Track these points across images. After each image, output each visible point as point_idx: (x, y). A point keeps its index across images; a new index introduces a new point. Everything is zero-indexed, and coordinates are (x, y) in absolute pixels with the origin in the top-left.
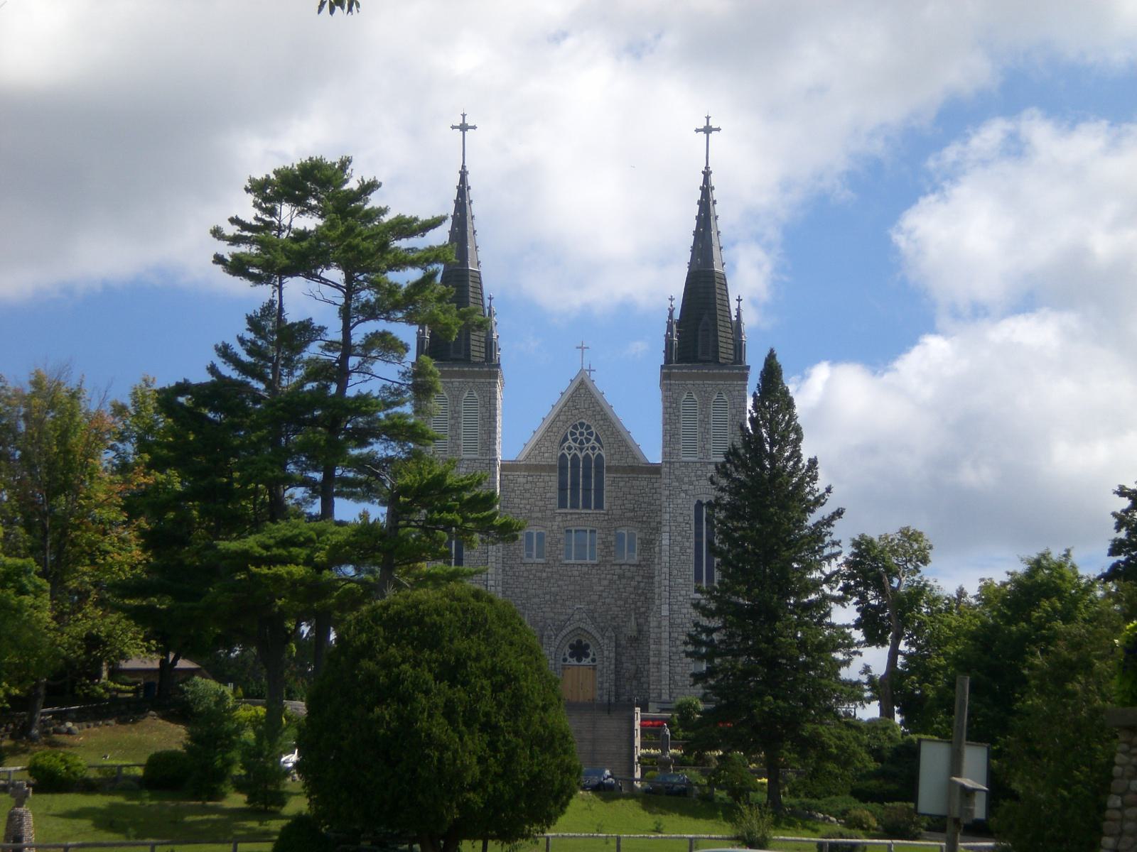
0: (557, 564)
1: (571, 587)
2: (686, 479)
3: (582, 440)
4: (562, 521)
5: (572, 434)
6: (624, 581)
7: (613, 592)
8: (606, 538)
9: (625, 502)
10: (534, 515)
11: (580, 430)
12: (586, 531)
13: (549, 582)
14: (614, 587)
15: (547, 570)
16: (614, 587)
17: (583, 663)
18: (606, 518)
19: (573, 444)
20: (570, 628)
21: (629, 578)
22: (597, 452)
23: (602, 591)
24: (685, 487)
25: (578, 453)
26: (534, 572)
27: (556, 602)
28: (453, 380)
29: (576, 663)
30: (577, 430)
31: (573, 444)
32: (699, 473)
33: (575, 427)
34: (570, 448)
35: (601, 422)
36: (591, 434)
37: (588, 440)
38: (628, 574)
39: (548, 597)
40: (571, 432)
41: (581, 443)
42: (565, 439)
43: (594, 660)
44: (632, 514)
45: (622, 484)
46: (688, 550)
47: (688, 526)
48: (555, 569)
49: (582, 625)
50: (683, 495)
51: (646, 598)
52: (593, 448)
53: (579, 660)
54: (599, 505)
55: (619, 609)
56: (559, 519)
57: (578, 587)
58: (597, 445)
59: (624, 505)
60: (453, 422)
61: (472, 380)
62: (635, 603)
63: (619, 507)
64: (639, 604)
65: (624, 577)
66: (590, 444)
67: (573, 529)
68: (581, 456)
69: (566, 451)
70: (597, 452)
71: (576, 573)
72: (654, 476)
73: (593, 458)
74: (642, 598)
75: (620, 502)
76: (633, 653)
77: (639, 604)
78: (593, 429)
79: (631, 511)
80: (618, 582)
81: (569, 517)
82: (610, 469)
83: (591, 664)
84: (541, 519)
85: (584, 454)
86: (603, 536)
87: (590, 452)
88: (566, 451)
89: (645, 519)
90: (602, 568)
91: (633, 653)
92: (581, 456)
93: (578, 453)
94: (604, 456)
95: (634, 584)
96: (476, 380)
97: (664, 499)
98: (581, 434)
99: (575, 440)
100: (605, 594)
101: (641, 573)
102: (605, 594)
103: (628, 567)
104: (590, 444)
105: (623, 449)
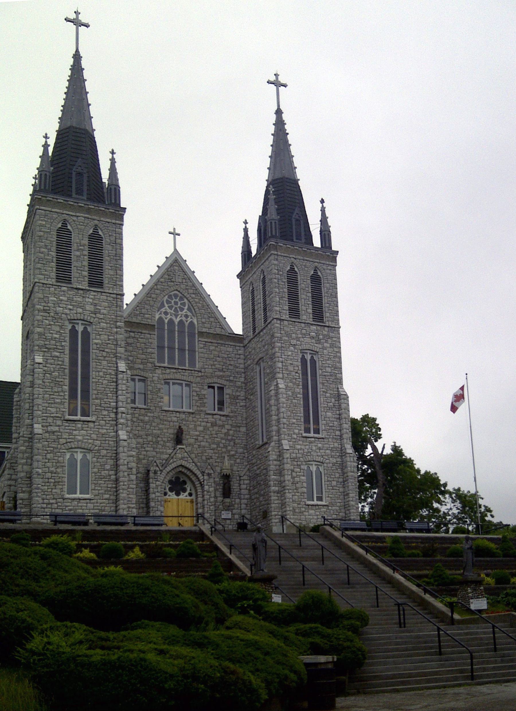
4: (162, 374)
5: (168, 302)
6: (216, 428)
8: (200, 392)
9: (215, 363)
10: (137, 366)
11: (174, 300)
13: (151, 425)
14: (208, 432)
15: (149, 414)
16: (208, 432)
18: (200, 374)
19: (169, 310)
21: (220, 426)
22: (189, 320)
23: (198, 436)
26: (137, 415)
27: (157, 442)
28: (78, 214)
34: (166, 313)
35: (193, 296)
37: (182, 310)
39: (150, 438)
40: (167, 300)
41: (176, 310)
42: (163, 305)
44: (221, 373)
45: (212, 348)
47: (297, 374)
48: (156, 414)
49: (184, 463)
52: (187, 316)
55: (212, 451)
58: (189, 314)
59: (214, 365)
60: (78, 253)
62: (225, 447)
63: (210, 367)
65: (216, 425)
66: (184, 312)
68: (177, 321)
69: (163, 316)
70: (189, 320)
72: (238, 344)
73: (187, 324)
74: (232, 443)
75: (212, 363)
79: (220, 371)
80: (211, 429)
81: (168, 371)
82: (201, 334)
84: (143, 370)
85: (178, 319)
86: (198, 389)
87: (184, 319)
89: (231, 378)
90: (198, 417)
92: (177, 321)
93: (174, 318)
94: (196, 323)
95: (224, 431)
98: (176, 303)
99: (170, 307)
100: (200, 438)
101: (230, 422)
103: (219, 416)
104: (184, 312)
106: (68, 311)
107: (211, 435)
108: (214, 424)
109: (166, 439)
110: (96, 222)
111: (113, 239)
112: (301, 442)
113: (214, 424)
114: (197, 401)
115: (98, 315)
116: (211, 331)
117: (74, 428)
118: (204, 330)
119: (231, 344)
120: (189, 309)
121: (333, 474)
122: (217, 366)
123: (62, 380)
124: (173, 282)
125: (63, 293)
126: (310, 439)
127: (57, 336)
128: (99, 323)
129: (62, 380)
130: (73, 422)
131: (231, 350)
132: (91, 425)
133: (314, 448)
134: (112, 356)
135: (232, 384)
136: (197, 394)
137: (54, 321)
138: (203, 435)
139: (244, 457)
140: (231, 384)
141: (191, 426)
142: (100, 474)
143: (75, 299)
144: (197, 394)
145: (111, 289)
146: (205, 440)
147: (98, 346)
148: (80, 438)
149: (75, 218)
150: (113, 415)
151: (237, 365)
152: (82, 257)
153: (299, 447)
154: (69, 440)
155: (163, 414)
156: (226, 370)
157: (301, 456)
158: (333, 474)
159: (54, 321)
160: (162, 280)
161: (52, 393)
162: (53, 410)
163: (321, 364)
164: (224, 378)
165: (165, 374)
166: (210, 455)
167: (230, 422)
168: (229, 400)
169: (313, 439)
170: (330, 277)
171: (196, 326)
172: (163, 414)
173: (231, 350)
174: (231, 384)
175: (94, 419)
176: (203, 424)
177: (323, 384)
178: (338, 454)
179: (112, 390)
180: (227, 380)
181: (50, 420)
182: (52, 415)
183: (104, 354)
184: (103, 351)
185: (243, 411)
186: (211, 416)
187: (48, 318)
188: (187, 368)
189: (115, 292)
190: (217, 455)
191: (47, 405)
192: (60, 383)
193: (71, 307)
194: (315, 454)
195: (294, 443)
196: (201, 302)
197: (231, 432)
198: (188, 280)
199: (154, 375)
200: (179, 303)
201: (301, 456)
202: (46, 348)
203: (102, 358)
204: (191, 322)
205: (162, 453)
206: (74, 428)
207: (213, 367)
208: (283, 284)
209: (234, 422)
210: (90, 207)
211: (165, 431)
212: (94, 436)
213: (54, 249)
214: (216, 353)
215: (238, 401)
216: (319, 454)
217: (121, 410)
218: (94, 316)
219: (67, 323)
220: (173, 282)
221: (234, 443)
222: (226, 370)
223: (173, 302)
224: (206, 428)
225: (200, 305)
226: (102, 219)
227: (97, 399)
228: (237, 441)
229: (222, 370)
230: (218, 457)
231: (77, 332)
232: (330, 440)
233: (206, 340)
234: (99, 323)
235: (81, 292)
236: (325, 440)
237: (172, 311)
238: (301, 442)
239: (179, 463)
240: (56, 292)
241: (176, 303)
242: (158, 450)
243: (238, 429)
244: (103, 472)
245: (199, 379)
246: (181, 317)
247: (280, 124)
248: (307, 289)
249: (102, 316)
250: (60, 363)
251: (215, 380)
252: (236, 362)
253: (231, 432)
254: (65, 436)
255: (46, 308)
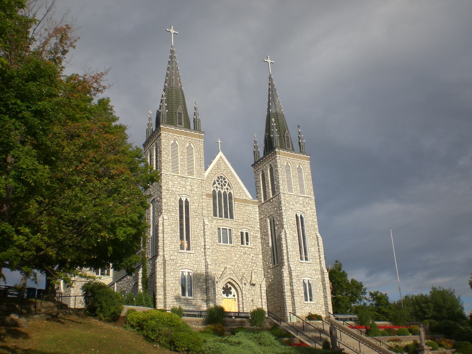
0: (215, 244)
1: (222, 257)
2: (291, 203)
3: (222, 184)
5: (218, 181)
6: (246, 256)
7: (241, 261)
8: (237, 233)
9: (244, 216)
11: (221, 179)
12: (226, 229)
16: (242, 258)
17: (229, 297)
19: (218, 186)
20: (226, 278)
21: (248, 254)
22: (229, 191)
24: (291, 207)
25: (221, 190)
28: (181, 136)
29: (226, 297)
30: (220, 179)
31: (218, 186)
32: (296, 200)
33: (218, 178)
34: (217, 187)
35: (231, 177)
36: (225, 182)
37: (225, 185)
38: (248, 252)
40: (217, 180)
41: (222, 186)
42: (214, 183)
43: (234, 296)
44: (247, 223)
45: (241, 208)
46: (296, 238)
50: (291, 210)
51: (256, 264)
52: (227, 189)
53: (227, 295)
54: (232, 217)
55: (245, 270)
56: (215, 221)
57: (225, 258)
58: (229, 187)
61: (191, 138)
64: (254, 268)
66: (226, 187)
67: (221, 227)
68: (222, 192)
69: (215, 189)
71: (224, 250)
73: (228, 194)
74: (255, 265)
76: (253, 292)
77: (254, 268)
78: (226, 180)
81: (219, 221)
83: (233, 297)
85: (223, 191)
86: (235, 232)
87: (226, 190)
88: (215, 189)
89: (253, 226)
91: (253, 292)
92: (222, 192)
93: (221, 190)
94: (232, 193)
95: (251, 257)
96: (193, 138)
97: (283, 211)
98: (222, 181)
99: (219, 184)
101: (253, 252)
102: (238, 262)
103: (247, 248)
104: (226, 187)
105: (241, 191)
106: (178, 190)
107: (244, 259)
108: (245, 253)
109: (220, 262)
110: (190, 140)
111: (198, 149)
112: (299, 266)
113: (245, 253)
114: (235, 239)
115: (193, 192)
116: (241, 198)
117: (184, 257)
118: (237, 197)
119: (251, 205)
120: (228, 185)
121: (317, 285)
122: (245, 218)
123: (177, 229)
124: (220, 169)
125: (175, 179)
126: (304, 264)
127: (173, 204)
128: (194, 196)
129: (177, 229)
130: (183, 254)
131: (251, 209)
132: (192, 255)
133: (306, 269)
134: (200, 215)
135: (253, 229)
136: (235, 235)
137: (172, 195)
138: (239, 260)
139: (262, 273)
140: (252, 229)
141: (233, 254)
142: (197, 285)
143: (181, 183)
144: (235, 235)
145: (199, 177)
146: (241, 263)
147: (194, 210)
148: (187, 263)
149: (180, 138)
150: (203, 250)
151: (255, 218)
152: (184, 159)
153: (298, 269)
154: (181, 264)
155: (218, 247)
156: (249, 221)
157: (300, 274)
158: (317, 285)
159: (172, 195)
160: (214, 168)
161: (172, 237)
162: (173, 247)
163: (306, 219)
164: (248, 226)
165: (218, 223)
166: (244, 272)
167: (253, 252)
168: (252, 239)
169: (305, 264)
170: (307, 169)
171: (233, 195)
172: (218, 247)
173: (251, 209)
174: (252, 229)
175: (193, 252)
176: (239, 253)
177: (308, 231)
178: (319, 273)
179: (201, 235)
180: (250, 227)
181: (172, 252)
182: (172, 249)
183: (197, 214)
184: (196, 212)
185: (259, 245)
186: (243, 248)
187: (169, 194)
188: (229, 220)
189: (201, 179)
190: (247, 272)
191: (170, 244)
192: (176, 231)
193: (180, 187)
194: (307, 273)
195: (296, 266)
196: (235, 181)
197: (254, 258)
198: (227, 169)
199: (212, 223)
200: (223, 181)
201: (300, 274)
202: (168, 211)
203: (196, 216)
204: (230, 193)
205: (218, 270)
206: (184, 257)
207: (243, 219)
208: (284, 173)
209: (255, 251)
210: (187, 131)
211: (219, 257)
212: (194, 262)
213: (170, 155)
214: (244, 211)
215: (256, 239)
216: (309, 273)
217: (207, 247)
218: (191, 192)
219: (178, 196)
220: (220, 169)
221: (256, 264)
222: (249, 221)
223: (223, 182)
224: (241, 256)
225: (234, 183)
226: (193, 138)
227: (194, 240)
228: (258, 264)
229: (247, 221)
230: (248, 273)
231: (182, 201)
232: (314, 264)
233: (239, 203)
234: (194, 196)
235: (184, 179)
236: (312, 264)
237: (220, 186)
238: (299, 266)
239: (229, 277)
240: (172, 179)
241: (222, 181)
242: (216, 269)
243: (258, 256)
244: (199, 283)
245: (235, 226)
246: (225, 189)
247: (271, 84)
248: (296, 176)
249: (195, 192)
250: (175, 219)
251: (244, 226)
252: (254, 216)
253: (254, 258)
254: (179, 262)
255: (167, 188)
